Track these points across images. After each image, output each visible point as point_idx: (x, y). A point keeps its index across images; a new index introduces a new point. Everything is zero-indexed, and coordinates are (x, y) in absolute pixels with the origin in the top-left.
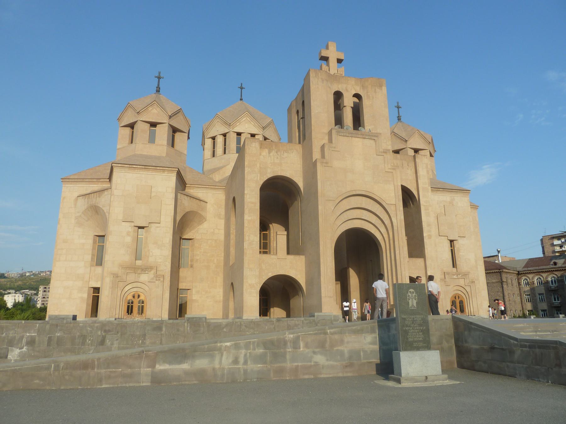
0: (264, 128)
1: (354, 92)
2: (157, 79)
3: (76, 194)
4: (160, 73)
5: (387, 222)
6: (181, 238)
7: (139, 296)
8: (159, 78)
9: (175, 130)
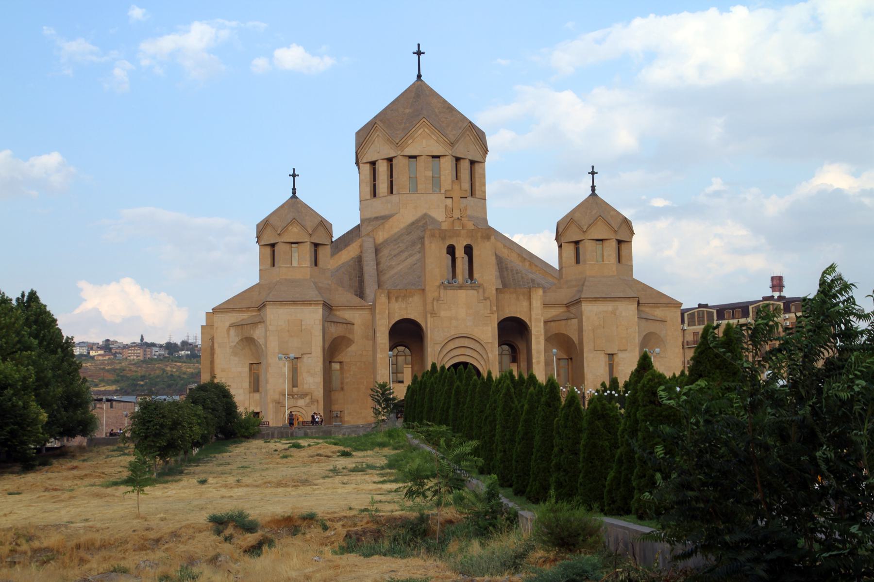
0: (452, 144)
1: (465, 243)
2: (292, 178)
3: (227, 324)
4: (294, 170)
5: (485, 357)
6: (330, 362)
7: (298, 420)
8: (294, 176)
9: (316, 245)
